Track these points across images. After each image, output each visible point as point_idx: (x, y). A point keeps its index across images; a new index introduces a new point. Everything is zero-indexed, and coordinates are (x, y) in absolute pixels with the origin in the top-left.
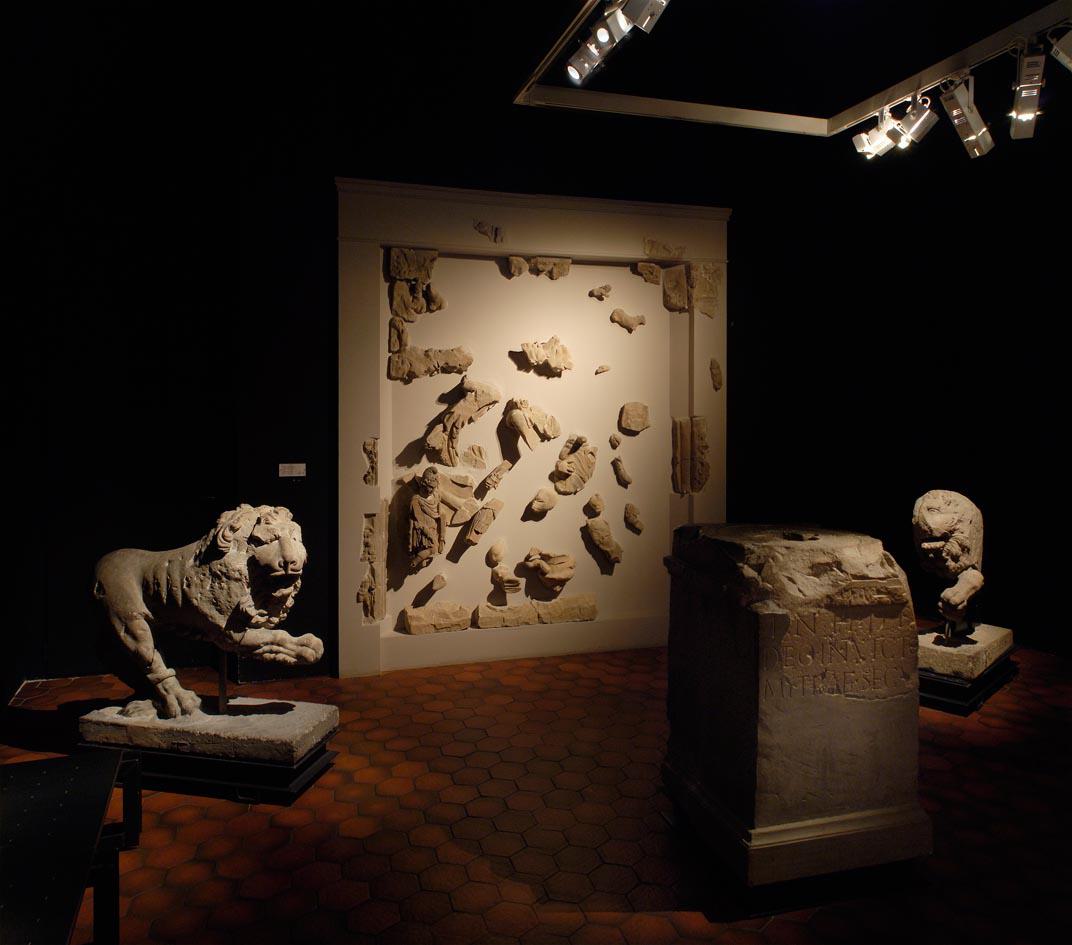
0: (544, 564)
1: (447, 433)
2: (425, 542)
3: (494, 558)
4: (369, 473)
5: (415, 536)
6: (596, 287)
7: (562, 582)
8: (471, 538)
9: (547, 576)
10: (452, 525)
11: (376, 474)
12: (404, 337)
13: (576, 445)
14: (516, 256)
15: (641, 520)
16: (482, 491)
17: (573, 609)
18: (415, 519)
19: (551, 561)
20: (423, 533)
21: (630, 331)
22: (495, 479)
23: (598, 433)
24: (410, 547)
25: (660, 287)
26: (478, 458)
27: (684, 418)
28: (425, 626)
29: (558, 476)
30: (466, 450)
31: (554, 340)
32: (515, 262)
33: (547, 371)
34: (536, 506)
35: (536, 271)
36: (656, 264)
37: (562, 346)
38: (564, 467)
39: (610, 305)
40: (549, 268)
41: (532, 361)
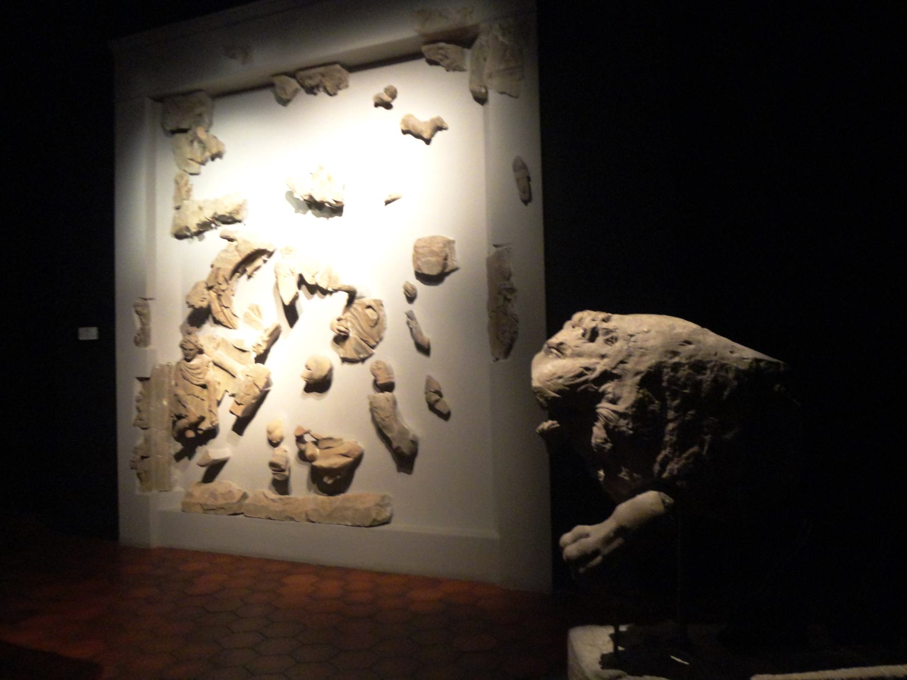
17: (347, 509)
21: (428, 142)
28: (194, 504)
36: (448, 41)
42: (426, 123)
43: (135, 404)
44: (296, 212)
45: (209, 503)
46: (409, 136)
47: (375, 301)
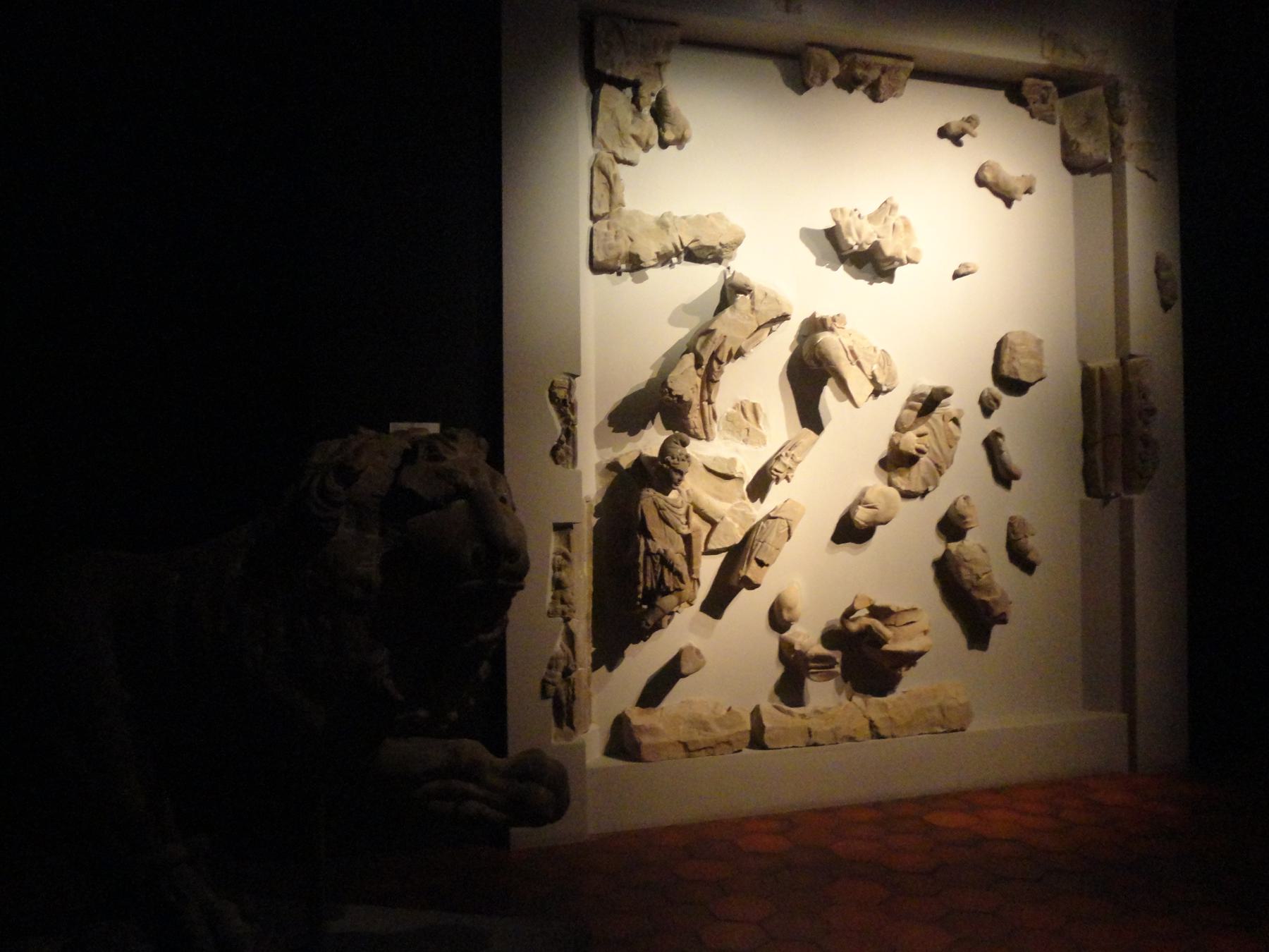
0: (877, 624)
1: (701, 372)
2: (669, 579)
3: (786, 615)
4: (560, 442)
5: (649, 567)
6: (954, 116)
7: (910, 659)
8: (749, 575)
9: (886, 647)
10: (708, 552)
11: (574, 444)
12: (617, 189)
13: (929, 403)
14: (821, 45)
15: (1035, 544)
16: (760, 486)
18: (648, 535)
19: (892, 620)
20: (665, 562)
22: (787, 461)
23: (969, 380)
24: (641, 588)
25: (1055, 131)
26: (752, 425)
27: (1107, 361)
29: (896, 460)
30: (730, 410)
31: (888, 207)
32: (817, 57)
33: (873, 264)
34: (862, 515)
35: (848, 83)
37: (903, 218)
38: (910, 441)
39: (974, 153)
40: (874, 74)
41: (851, 241)
42: (1018, 179)
43: (551, 571)
44: (819, 263)
45: (700, 738)
46: (985, 191)
47: (960, 411)
